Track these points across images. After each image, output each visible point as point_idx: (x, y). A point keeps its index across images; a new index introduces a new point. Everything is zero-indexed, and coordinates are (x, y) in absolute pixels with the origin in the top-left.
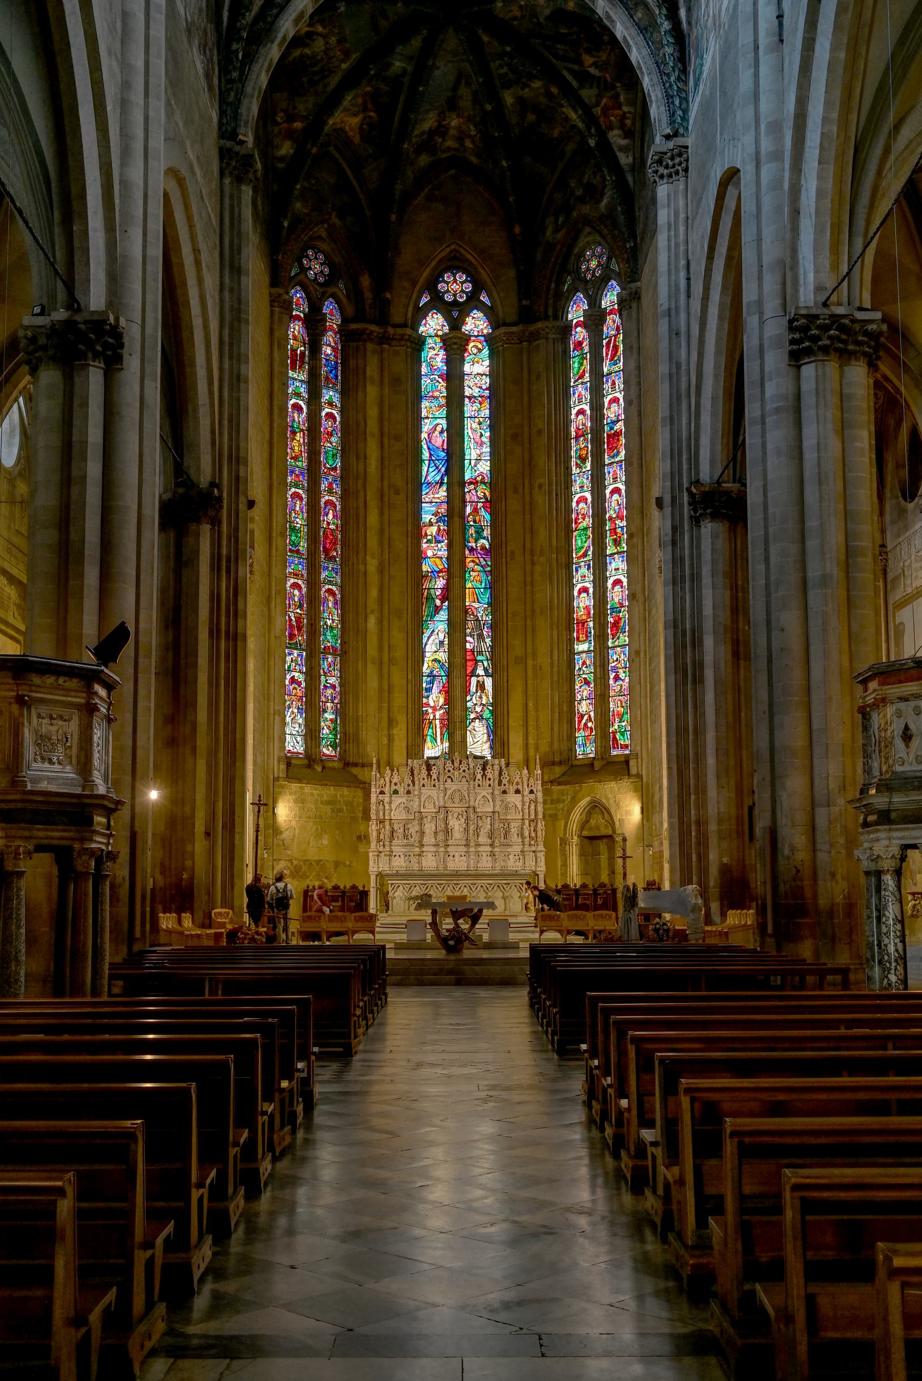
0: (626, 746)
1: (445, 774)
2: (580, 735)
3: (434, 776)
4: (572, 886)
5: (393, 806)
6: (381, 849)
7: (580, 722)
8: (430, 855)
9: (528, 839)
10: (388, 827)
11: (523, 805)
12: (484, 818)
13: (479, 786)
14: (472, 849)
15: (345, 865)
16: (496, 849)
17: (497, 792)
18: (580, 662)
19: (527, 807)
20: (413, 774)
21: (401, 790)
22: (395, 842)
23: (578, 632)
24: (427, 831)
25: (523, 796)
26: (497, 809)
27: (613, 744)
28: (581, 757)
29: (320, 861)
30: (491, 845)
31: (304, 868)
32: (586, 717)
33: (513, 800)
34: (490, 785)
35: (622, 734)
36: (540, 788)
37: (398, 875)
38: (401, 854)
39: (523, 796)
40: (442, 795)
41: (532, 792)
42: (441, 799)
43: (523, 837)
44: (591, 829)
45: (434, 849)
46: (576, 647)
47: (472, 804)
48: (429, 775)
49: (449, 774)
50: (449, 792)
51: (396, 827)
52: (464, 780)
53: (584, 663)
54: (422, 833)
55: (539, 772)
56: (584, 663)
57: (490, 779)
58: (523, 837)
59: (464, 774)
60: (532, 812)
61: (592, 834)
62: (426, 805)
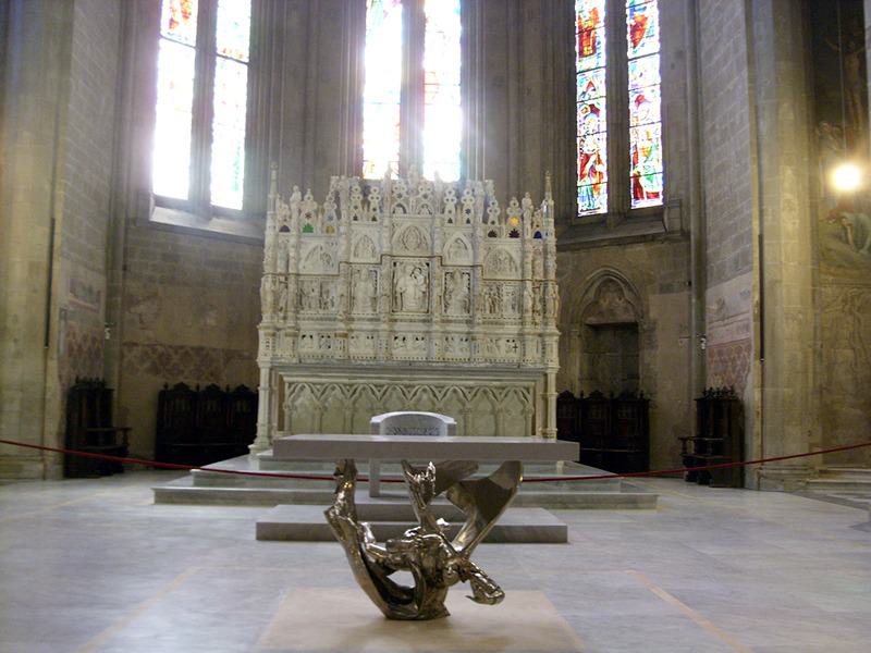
0: (656, 195)
1: (393, 200)
2: (584, 184)
3: (374, 203)
4: (577, 395)
5: (304, 253)
6: (280, 323)
7: (583, 166)
8: (363, 336)
9: (530, 314)
10: (292, 287)
11: (524, 257)
12: (458, 275)
13: (450, 221)
14: (436, 327)
15: (241, 357)
16: (477, 329)
17: (481, 232)
18: (586, 83)
19: (530, 259)
20: (337, 200)
21: (317, 227)
22: (306, 312)
23: (581, 44)
24: (360, 295)
25: (523, 242)
26: (480, 260)
27: (635, 193)
28: (584, 214)
29: (202, 349)
30: (467, 322)
31: (176, 359)
32: (593, 158)
33: (507, 248)
34: (468, 222)
35: (649, 176)
36: (552, 228)
37: (301, 366)
38: (314, 334)
39: (523, 242)
40: (387, 235)
41: (538, 235)
42: (385, 243)
43: (521, 308)
44: (601, 313)
45: (369, 326)
46: (578, 64)
47: (437, 251)
48: (366, 202)
49: (400, 201)
50: (398, 231)
51: (306, 288)
52: (425, 210)
53: (591, 84)
54: (352, 299)
55: (551, 203)
56: (591, 84)
57: (468, 211)
58: (521, 308)
59: (425, 201)
60: (540, 270)
61: (602, 321)
62: (360, 251)
